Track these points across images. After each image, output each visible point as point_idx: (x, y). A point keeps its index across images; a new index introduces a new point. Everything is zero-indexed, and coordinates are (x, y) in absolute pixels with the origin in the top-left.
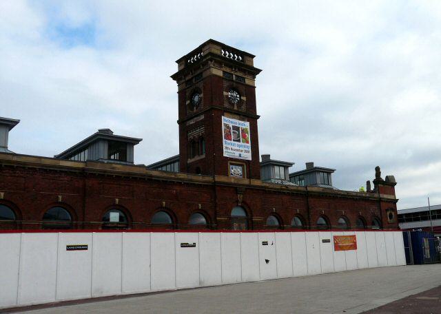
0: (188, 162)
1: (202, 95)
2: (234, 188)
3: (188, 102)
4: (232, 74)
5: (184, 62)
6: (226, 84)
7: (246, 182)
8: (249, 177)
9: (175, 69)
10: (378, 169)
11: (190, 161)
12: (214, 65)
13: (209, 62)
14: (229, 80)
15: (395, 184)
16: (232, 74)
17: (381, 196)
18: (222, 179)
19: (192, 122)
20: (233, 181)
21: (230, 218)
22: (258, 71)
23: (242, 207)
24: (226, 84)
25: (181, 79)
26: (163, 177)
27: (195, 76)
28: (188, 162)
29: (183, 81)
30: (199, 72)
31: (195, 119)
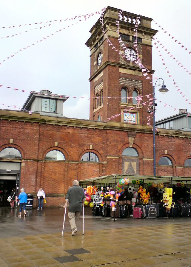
2: (129, 131)
4: (129, 36)
7: (140, 127)
12: (111, 28)
16: (129, 36)
20: (125, 126)
23: (132, 147)
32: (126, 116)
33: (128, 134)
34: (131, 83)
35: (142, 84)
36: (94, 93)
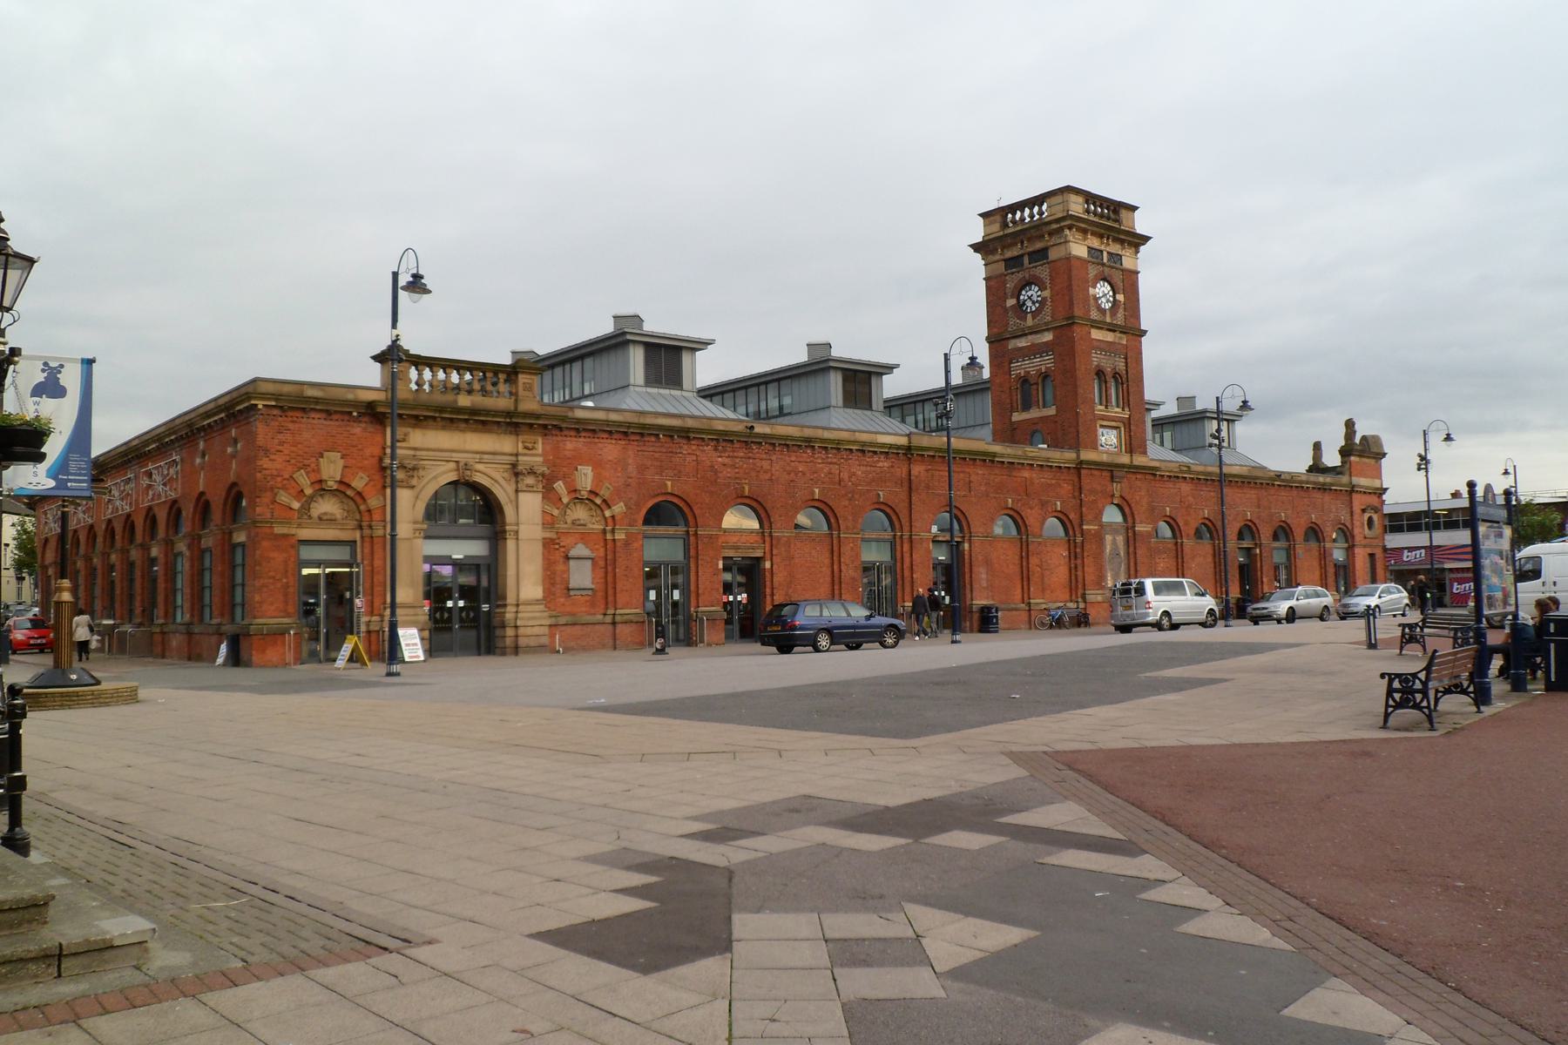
0: (1014, 419)
1: (1047, 293)
2: (1111, 470)
3: (1011, 302)
4: (1102, 251)
5: (998, 218)
6: (1093, 271)
7: (1125, 459)
8: (1131, 450)
9: (978, 233)
10: (1350, 424)
11: (1016, 417)
13: (1067, 232)
14: (1098, 264)
15: (1384, 455)
16: (1102, 251)
17: (1355, 480)
18: (1087, 455)
19: (1022, 343)
20: (1105, 458)
21: (1101, 525)
22: (1145, 239)
24: (1093, 271)
25: (993, 252)
26: (1009, 456)
27: (1030, 254)
28: (1014, 419)
29: (997, 257)
30: (1039, 245)
31: (1030, 337)
32: (1103, 435)
33: (1112, 477)
34: (1109, 360)
35: (1126, 363)
36: (1010, 375)
